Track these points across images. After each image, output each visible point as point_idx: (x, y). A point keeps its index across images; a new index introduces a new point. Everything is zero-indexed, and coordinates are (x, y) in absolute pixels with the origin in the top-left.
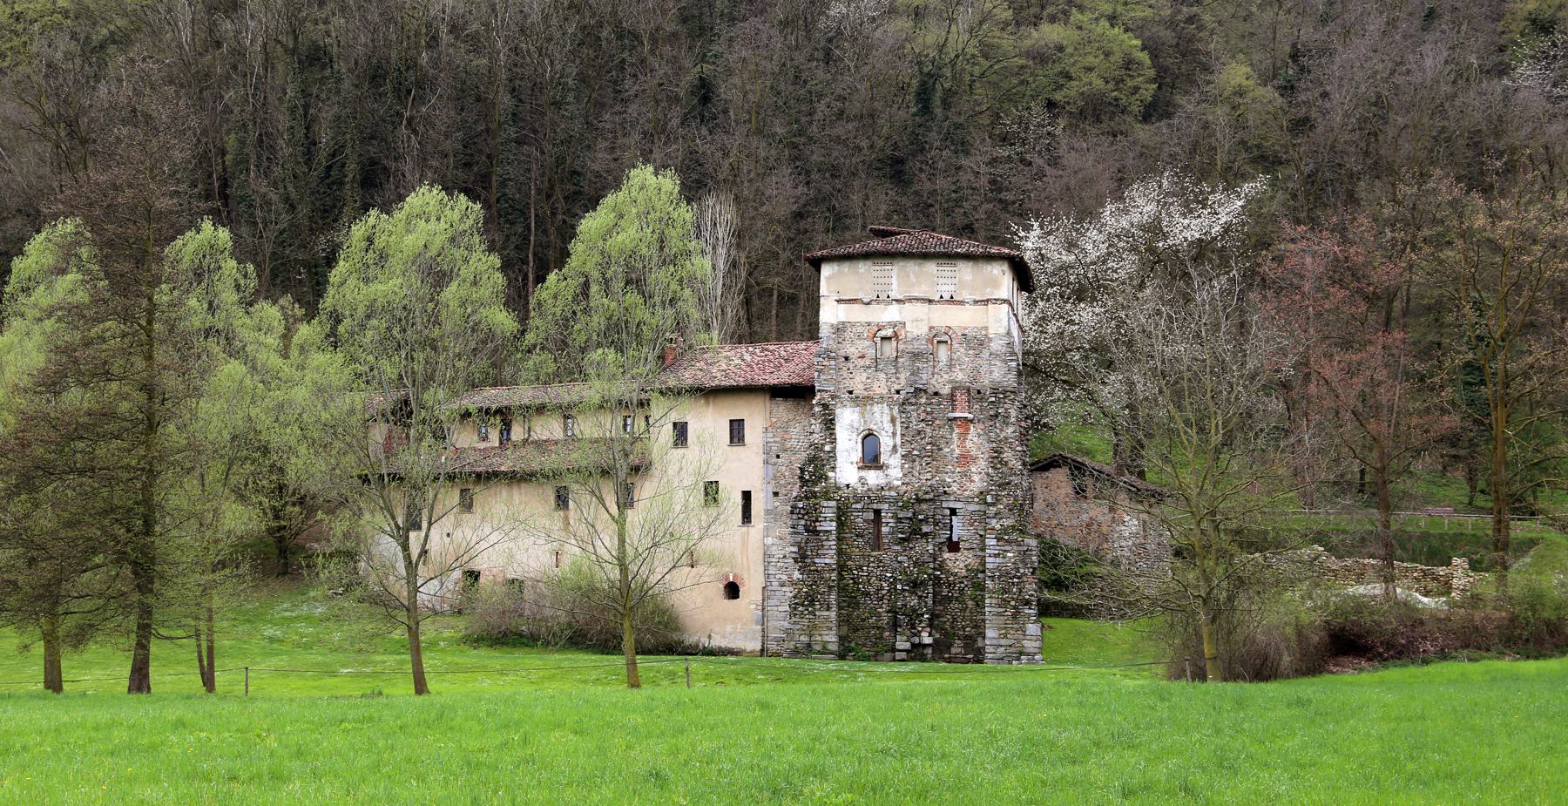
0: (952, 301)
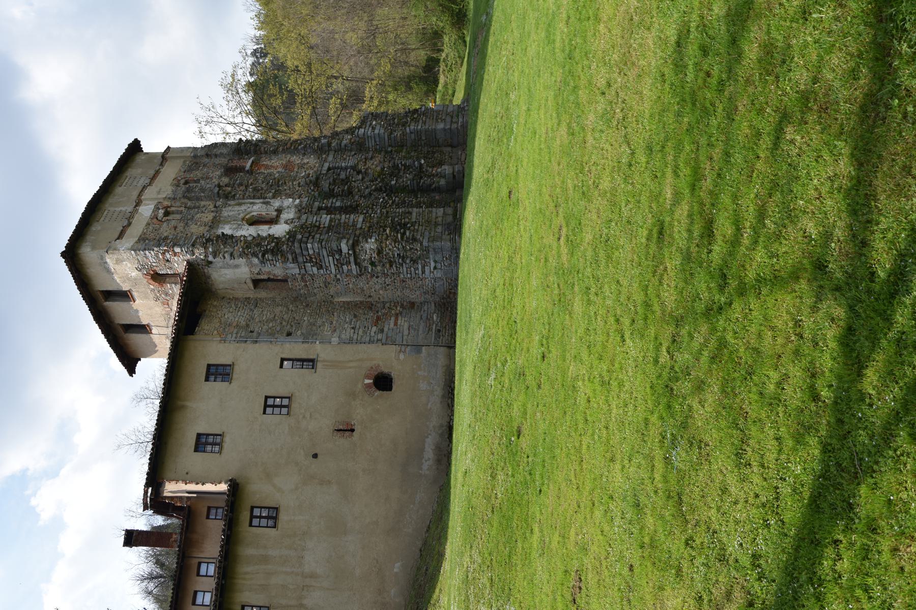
0: (153, 178)
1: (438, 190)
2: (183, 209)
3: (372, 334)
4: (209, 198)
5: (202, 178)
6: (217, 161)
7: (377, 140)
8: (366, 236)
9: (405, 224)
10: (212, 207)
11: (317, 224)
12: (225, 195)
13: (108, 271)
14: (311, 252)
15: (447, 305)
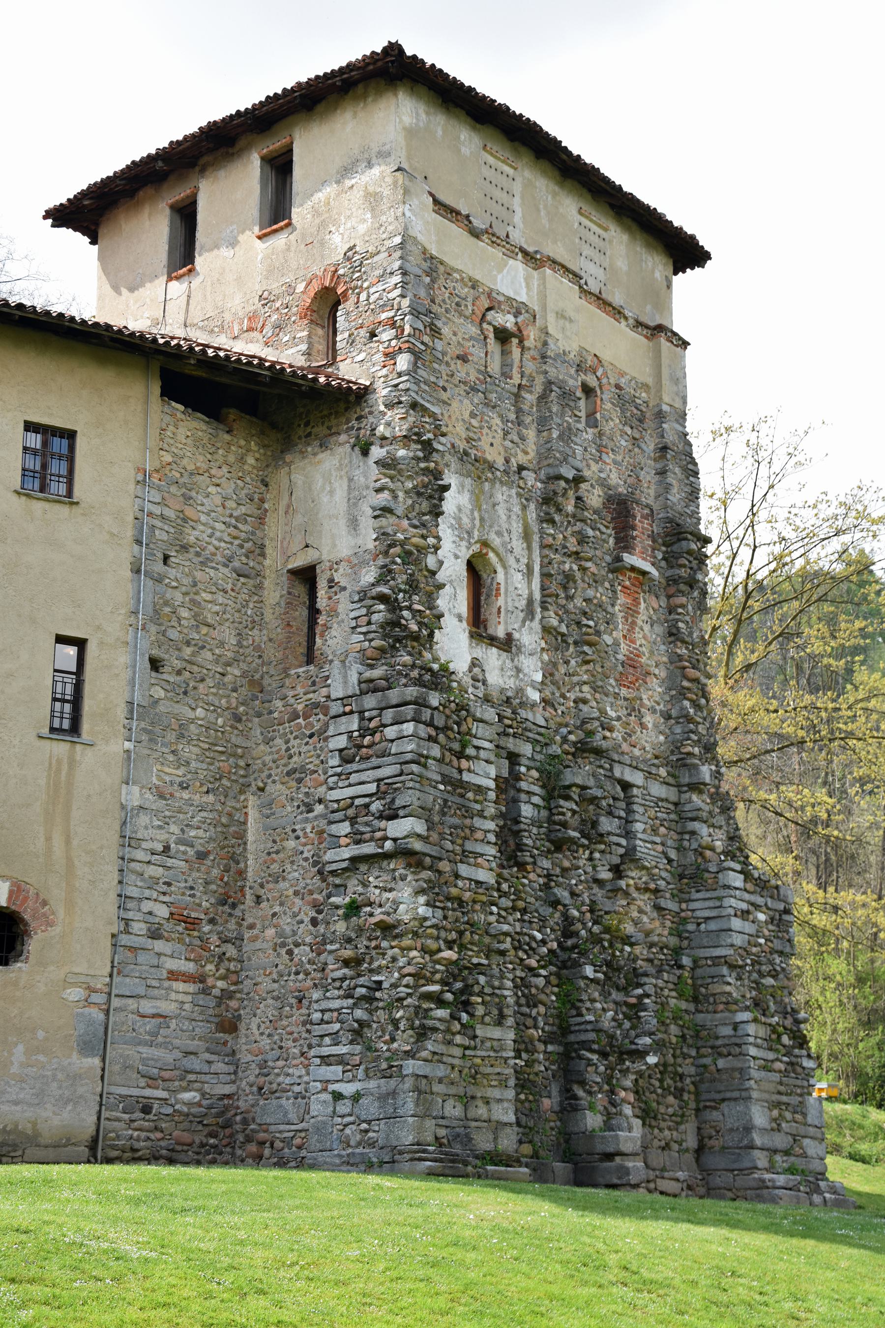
1: (570, 1106)
2: (516, 380)
3: (147, 906)
4: (545, 453)
5: (601, 434)
6: (648, 476)
7: (713, 926)
8: (433, 892)
9: (466, 1006)
10: (522, 459)
11: (470, 751)
12: (553, 497)
13: (347, 171)
14: (391, 732)
15: (223, 1136)
